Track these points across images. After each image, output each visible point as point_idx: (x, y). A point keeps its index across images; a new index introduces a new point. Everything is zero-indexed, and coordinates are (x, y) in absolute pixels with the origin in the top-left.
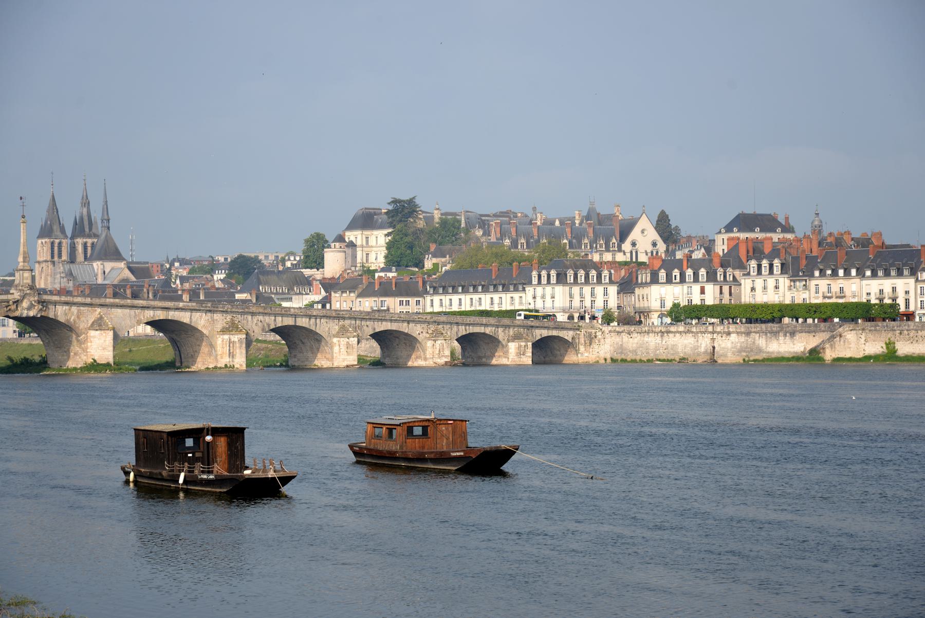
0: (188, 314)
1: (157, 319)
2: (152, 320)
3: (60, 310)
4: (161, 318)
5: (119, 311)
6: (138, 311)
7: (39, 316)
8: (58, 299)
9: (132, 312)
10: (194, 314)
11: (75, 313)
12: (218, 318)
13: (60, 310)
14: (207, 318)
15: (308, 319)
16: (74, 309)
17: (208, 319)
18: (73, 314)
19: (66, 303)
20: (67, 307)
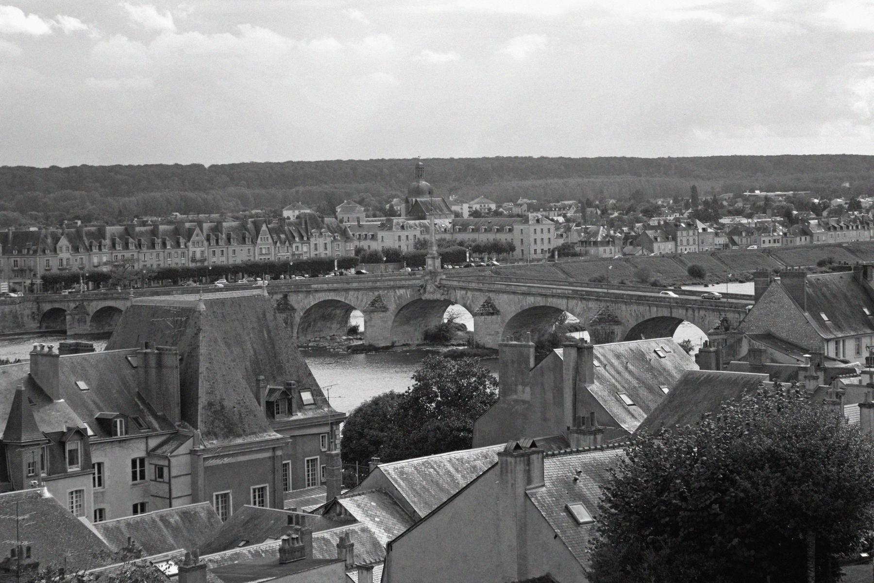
0: (565, 301)
1: (538, 305)
2: (533, 306)
3: (459, 294)
4: (541, 305)
5: (505, 296)
6: (521, 297)
7: (442, 299)
8: (457, 284)
9: (516, 298)
10: (570, 301)
11: (470, 297)
12: (593, 306)
13: (459, 294)
14: (582, 306)
15: (685, 311)
16: (470, 294)
17: (584, 307)
18: (468, 298)
19: (462, 288)
20: (463, 292)
